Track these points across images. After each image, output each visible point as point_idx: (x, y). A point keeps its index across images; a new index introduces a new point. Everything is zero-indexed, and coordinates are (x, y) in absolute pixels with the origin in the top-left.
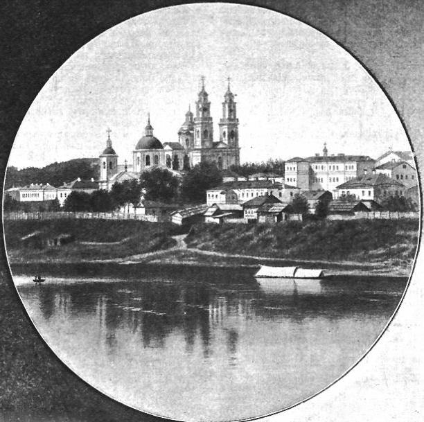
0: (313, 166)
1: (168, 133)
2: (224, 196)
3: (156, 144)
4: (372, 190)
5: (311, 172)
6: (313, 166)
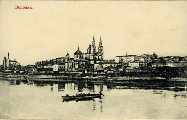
0: (123, 58)
1: (84, 50)
2: (99, 66)
3: (80, 53)
4: (138, 64)
5: (122, 59)
6: (123, 58)
